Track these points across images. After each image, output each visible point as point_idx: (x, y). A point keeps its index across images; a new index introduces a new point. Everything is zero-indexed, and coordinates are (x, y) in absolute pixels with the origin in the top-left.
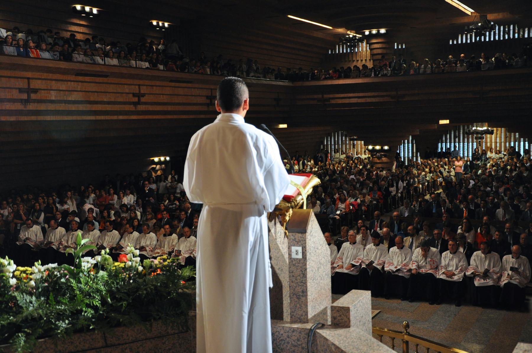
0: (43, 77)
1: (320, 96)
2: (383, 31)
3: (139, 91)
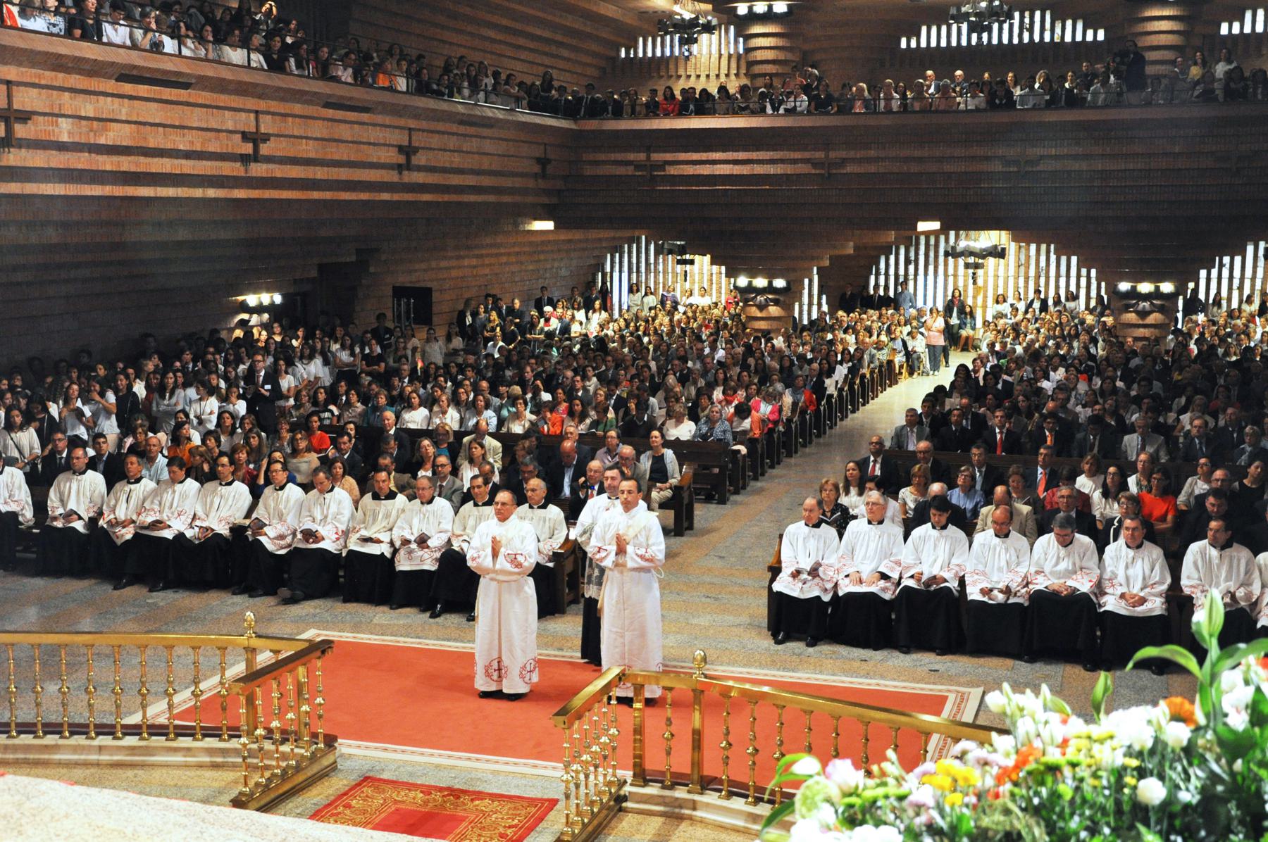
0: (43, 82)
1: (642, 156)
3: (257, 126)
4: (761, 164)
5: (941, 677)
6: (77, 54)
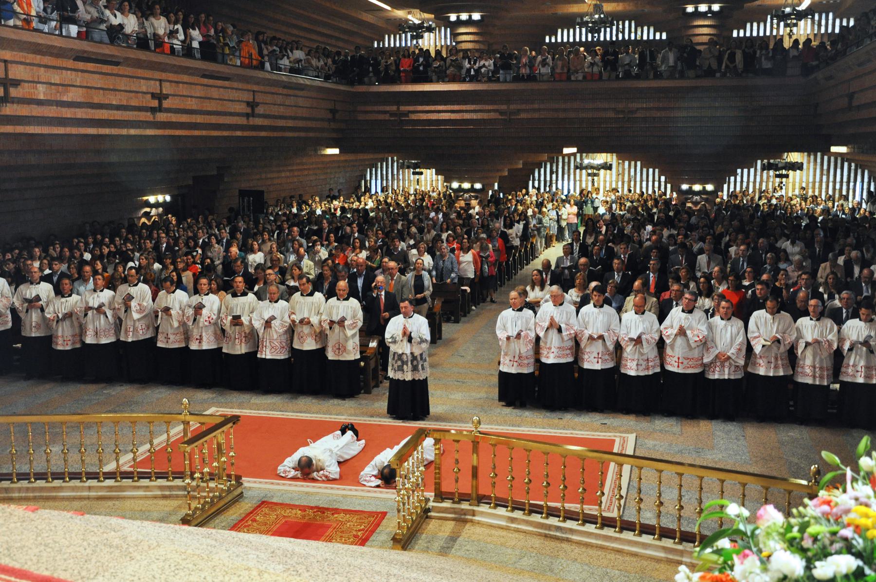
0: (28, 61)
1: (394, 108)
2: (476, 16)
3: (161, 90)
4: (469, 113)
5: (609, 427)
6: (50, 43)
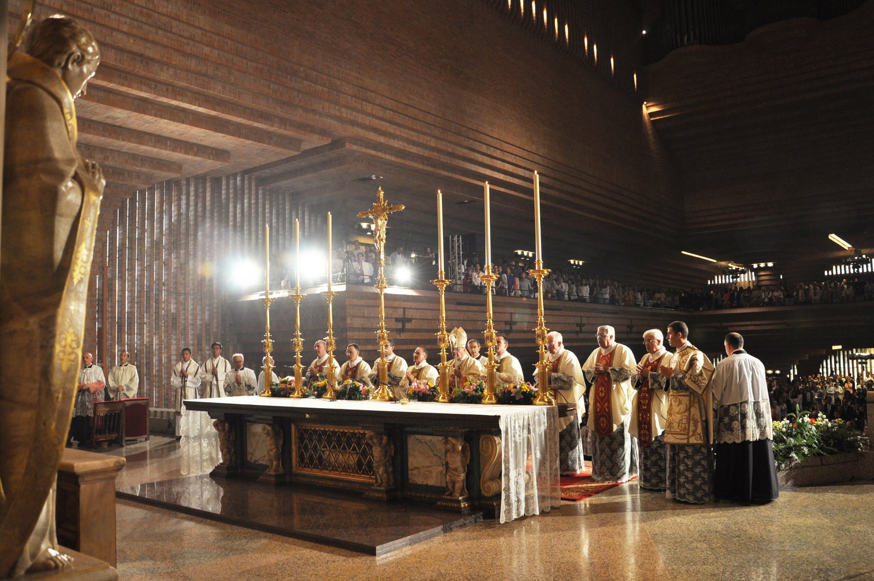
1: (718, 324)
2: (770, 264)
